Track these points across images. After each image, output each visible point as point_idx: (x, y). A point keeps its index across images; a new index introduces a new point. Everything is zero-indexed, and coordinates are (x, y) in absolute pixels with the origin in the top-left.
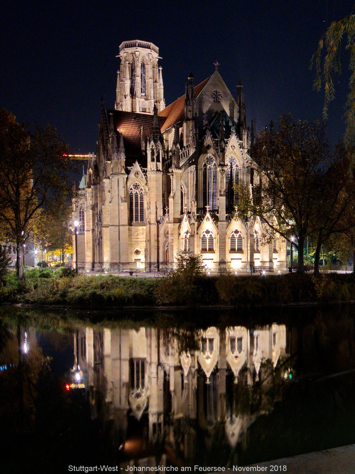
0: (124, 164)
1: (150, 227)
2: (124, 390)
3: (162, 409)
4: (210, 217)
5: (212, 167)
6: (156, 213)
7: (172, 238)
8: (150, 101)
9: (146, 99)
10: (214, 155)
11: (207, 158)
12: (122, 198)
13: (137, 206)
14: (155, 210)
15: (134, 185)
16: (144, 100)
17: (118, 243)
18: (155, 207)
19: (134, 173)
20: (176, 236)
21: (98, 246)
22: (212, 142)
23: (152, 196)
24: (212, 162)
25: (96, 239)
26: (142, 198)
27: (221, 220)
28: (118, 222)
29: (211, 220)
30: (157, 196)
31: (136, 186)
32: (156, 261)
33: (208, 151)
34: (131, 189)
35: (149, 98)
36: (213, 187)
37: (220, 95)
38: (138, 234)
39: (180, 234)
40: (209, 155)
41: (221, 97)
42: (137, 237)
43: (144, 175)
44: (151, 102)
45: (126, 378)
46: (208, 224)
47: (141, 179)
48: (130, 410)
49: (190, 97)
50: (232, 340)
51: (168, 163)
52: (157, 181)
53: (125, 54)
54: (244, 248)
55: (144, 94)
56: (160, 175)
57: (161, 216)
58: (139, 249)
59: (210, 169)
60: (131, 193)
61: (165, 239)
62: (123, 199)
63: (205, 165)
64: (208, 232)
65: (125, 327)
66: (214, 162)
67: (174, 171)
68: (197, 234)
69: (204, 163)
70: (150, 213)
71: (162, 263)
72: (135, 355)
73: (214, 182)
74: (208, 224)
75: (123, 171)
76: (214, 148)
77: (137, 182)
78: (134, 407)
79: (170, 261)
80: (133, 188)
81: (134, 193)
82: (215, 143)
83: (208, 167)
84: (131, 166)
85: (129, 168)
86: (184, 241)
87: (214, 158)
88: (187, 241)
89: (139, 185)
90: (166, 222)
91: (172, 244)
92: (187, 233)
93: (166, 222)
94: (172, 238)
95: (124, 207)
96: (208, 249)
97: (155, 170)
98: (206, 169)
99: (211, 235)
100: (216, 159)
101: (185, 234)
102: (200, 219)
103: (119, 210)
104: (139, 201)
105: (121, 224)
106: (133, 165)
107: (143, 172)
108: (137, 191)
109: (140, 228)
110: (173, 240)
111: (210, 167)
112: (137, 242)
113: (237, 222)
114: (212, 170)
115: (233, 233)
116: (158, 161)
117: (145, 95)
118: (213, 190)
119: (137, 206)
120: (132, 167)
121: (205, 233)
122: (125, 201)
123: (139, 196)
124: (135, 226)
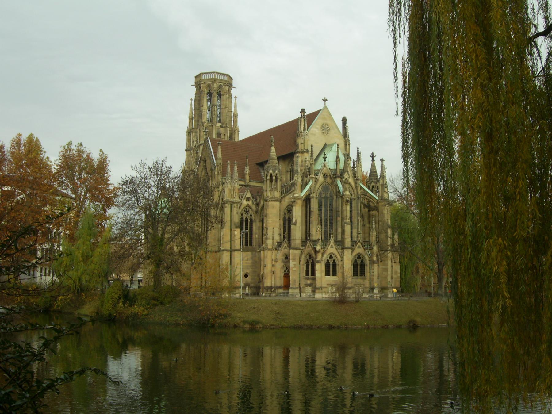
6: (273, 239)
18: (272, 232)
70: (266, 239)
76: (331, 178)
81: (244, 218)
123: (249, 220)
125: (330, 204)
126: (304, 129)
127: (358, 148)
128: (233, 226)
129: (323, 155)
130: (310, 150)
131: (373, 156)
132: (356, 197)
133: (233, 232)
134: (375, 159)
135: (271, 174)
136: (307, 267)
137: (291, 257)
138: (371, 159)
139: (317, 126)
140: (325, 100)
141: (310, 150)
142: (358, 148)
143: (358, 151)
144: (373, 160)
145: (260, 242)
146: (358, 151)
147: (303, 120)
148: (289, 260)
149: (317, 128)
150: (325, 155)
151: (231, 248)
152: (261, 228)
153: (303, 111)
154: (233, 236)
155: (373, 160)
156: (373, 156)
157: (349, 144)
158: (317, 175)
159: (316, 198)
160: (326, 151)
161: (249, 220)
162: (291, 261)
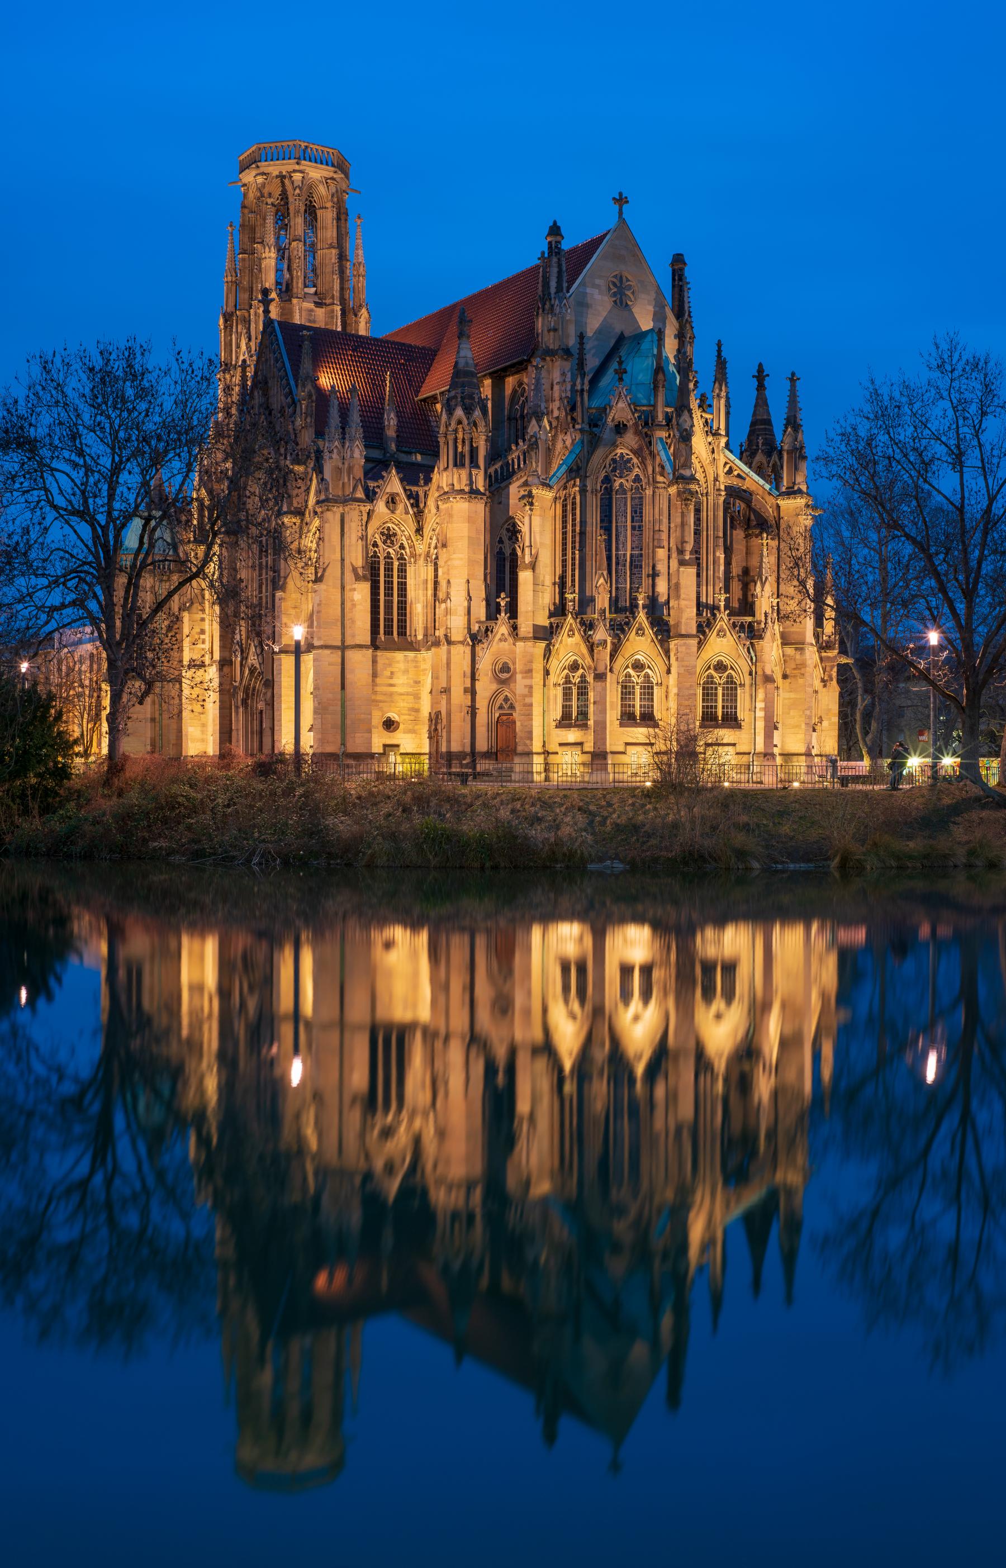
0: (359, 473)
1: (449, 652)
2: (354, 1117)
3: (478, 1168)
4: (646, 624)
5: (627, 485)
7: (527, 682)
8: (331, 307)
9: (319, 305)
10: (637, 453)
11: (614, 460)
12: (354, 570)
13: (389, 593)
14: (466, 604)
15: (382, 534)
16: (312, 306)
17: (339, 696)
18: (464, 594)
19: (384, 498)
20: (538, 677)
21: (241, 710)
22: (630, 416)
23: (456, 563)
24: (630, 470)
25: (235, 688)
26: (402, 571)
27: (683, 632)
28: (339, 637)
29: (649, 631)
30: (471, 563)
31: (389, 536)
32: (468, 749)
33: (619, 440)
34: (375, 545)
35: (328, 301)
36: (633, 541)
37: (630, 287)
38: (392, 673)
39: (547, 673)
40: (619, 451)
41: (633, 293)
42: (391, 682)
43: (412, 505)
44: (333, 311)
45: (359, 1078)
46: (641, 645)
47: (404, 516)
48: (368, 1176)
49: (553, 290)
50: (708, 968)
51: (496, 471)
52: (470, 520)
53: (260, 180)
54: (742, 713)
55: (313, 290)
56: (479, 508)
57: (479, 622)
58: (394, 716)
59: (622, 489)
60: (375, 555)
61: (494, 686)
62: (360, 572)
63: (607, 480)
64: (638, 666)
65: (625, 927)
66: (636, 471)
67: (534, 492)
68: (611, 670)
69: (603, 474)
70: (448, 612)
71: (487, 755)
72: (381, 1014)
73: (633, 528)
74: (641, 645)
75: (360, 494)
76: (637, 433)
77: (389, 525)
78: (379, 1164)
79: (520, 749)
80: (380, 543)
81: (382, 556)
82: (639, 417)
83: (616, 485)
84: (376, 480)
85: (372, 484)
86: (559, 691)
87: (635, 460)
88: (575, 691)
89: (395, 535)
90: (498, 636)
91: (527, 700)
92: (574, 667)
93: (498, 636)
94: (527, 682)
95: (360, 594)
96: (638, 714)
97: (467, 489)
98: (609, 491)
99: (647, 676)
100: (643, 462)
101: (566, 671)
102: (619, 630)
103: (343, 603)
104: (395, 580)
105: (339, 644)
106: (382, 477)
107: (409, 497)
108: (391, 550)
109: (399, 656)
110: (531, 687)
111: (621, 485)
112: (391, 694)
113: (724, 640)
114: (629, 495)
115: (712, 671)
116: (474, 463)
117: (316, 293)
118: (632, 549)
119: (389, 593)
120: (381, 482)
121: (630, 670)
122: (364, 578)
123: (396, 564)
124: (385, 649)
125: (634, 512)
126: (559, 289)
127: (719, 344)
128: (349, 576)
129: (615, 365)
130: (575, 351)
131: (761, 376)
132: (711, 490)
133: (348, 594)
134: (767, 382)
135: (460, 422)
136: (567, 695)
137: (519, 667)
138: (755, 383)
139: (597, 281)
140: (621, 200)
141: (575, 351)
142: (719, 344)
143: (719, 351)
144: (761, 387)
145: (430, 625)
146: (719, 351)
147: (555, 259)
148: (515, 673)
149: (598, 287)
150: (620, 363)
151: (343, 641)
152: (430, 586)
153: (555, 230)
154: (348, 605)
155: (761, 387)
156: (761, 376)
157: (693, 337)
158: (596, 426)
159: (594, 492)
160: (623, 352)
161: (396, 564)
162: (519, 677)
